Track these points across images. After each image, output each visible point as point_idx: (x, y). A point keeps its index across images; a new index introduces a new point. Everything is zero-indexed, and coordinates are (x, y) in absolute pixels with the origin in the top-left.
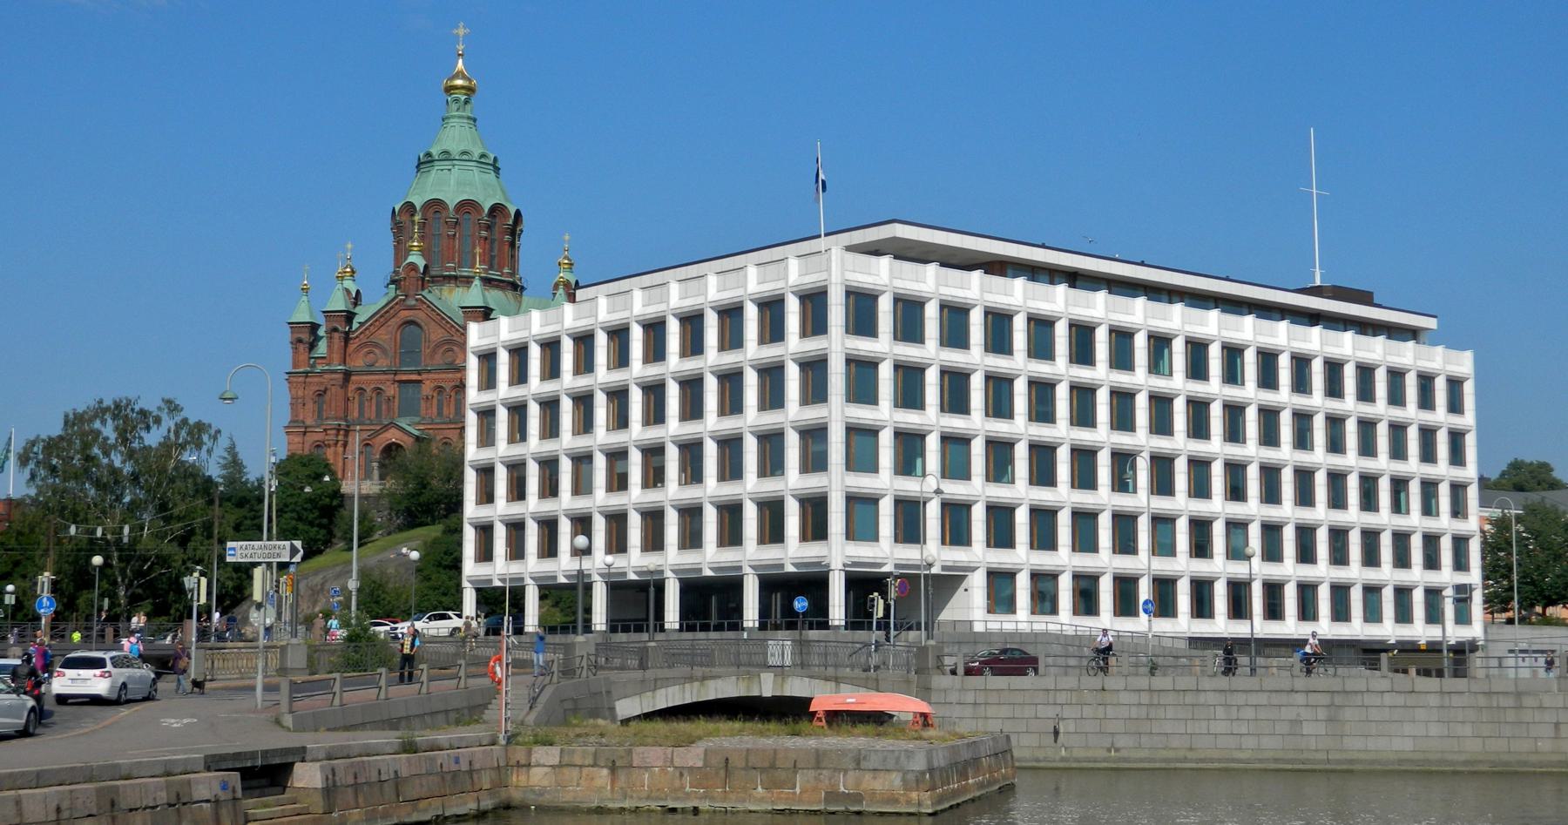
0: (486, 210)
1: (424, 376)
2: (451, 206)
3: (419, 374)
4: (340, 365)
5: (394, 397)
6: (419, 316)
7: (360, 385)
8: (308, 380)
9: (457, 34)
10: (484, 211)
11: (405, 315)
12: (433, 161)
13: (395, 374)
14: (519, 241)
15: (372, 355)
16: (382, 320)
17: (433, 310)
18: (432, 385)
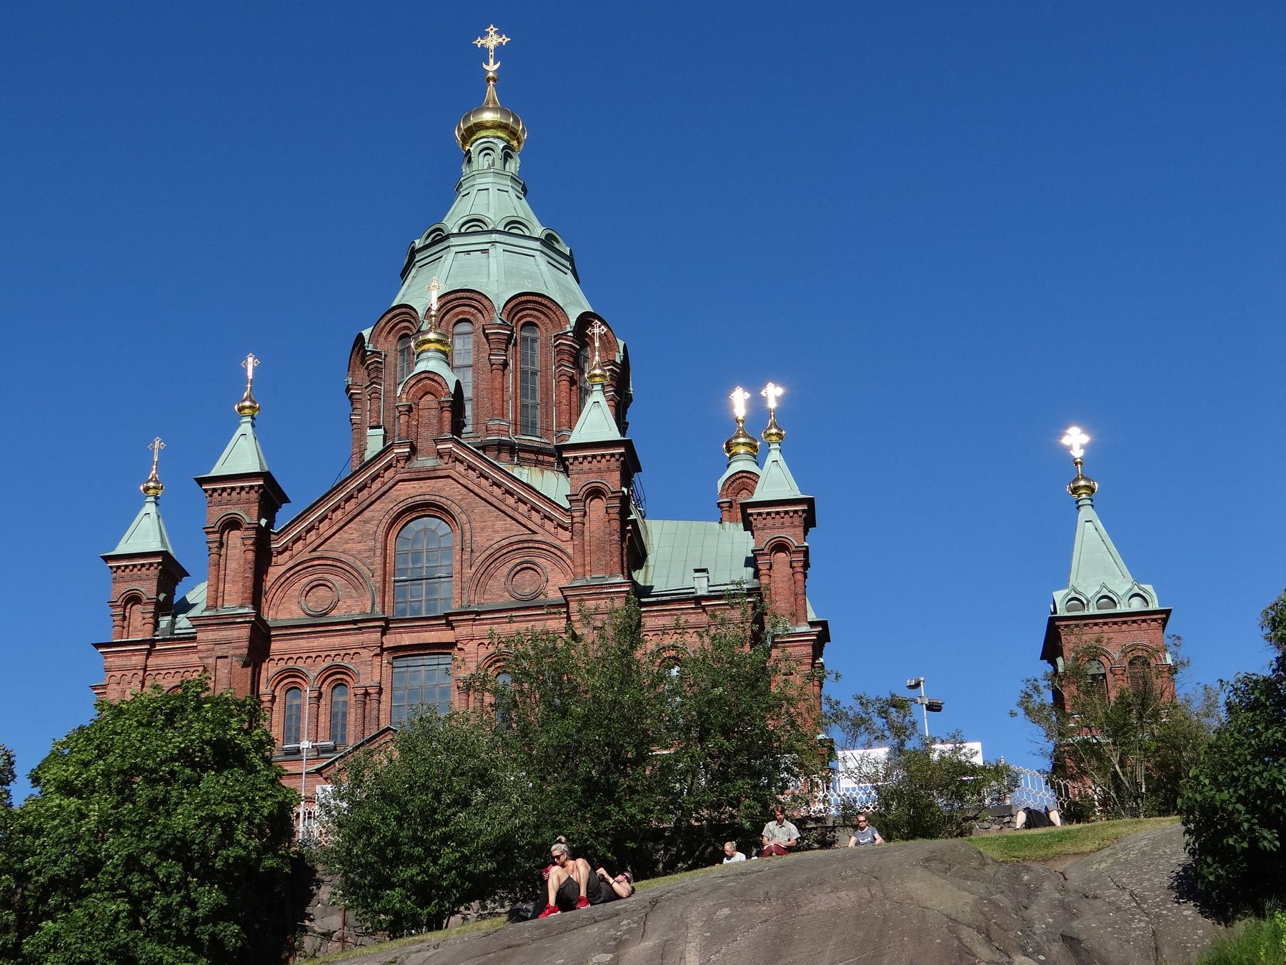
0: (573, 321)
1: (463, 630)
2: (499, 303)
3: (450, 625)
4: (242, 606)
5: (380, 692)
6: (445, 491)
7: (291, 664)
8: (152, 661)
9: (485, 50)
10: (568, 321)
11: (410, 492)
12: (447, 237)
13: (385, 631)
14: (624, 418)
15: (321, 591)
16: (350, 506)
17: (482, 475)
18: (483, 652)
